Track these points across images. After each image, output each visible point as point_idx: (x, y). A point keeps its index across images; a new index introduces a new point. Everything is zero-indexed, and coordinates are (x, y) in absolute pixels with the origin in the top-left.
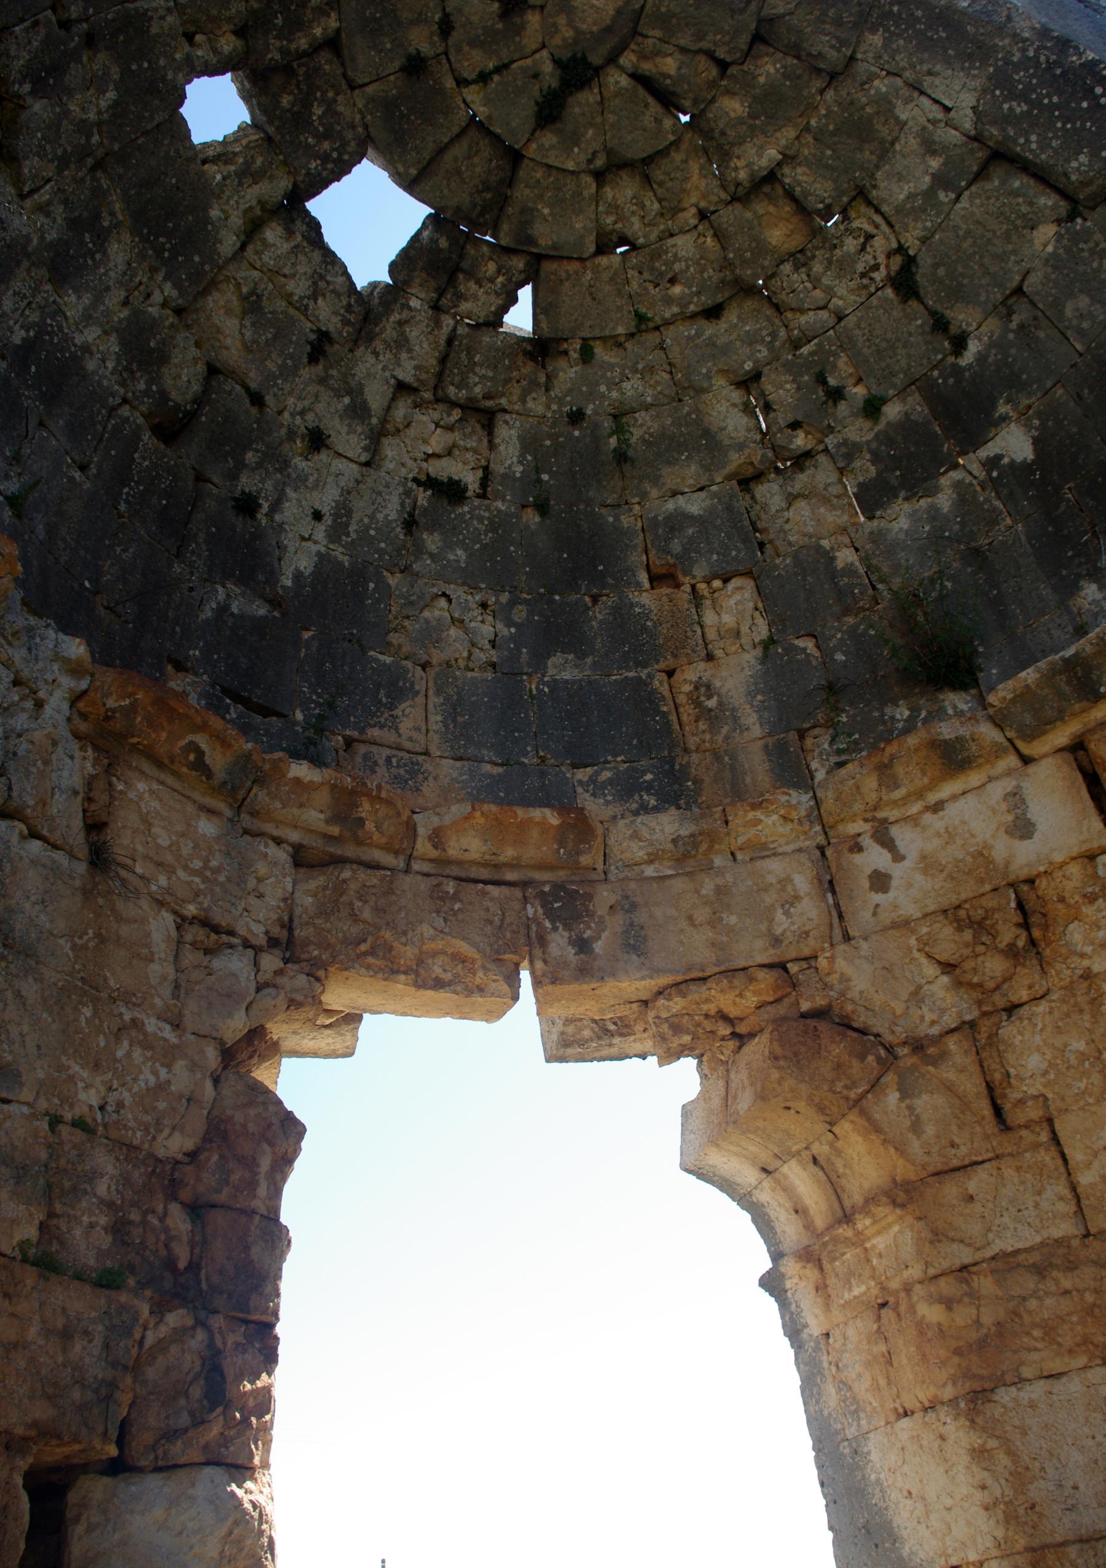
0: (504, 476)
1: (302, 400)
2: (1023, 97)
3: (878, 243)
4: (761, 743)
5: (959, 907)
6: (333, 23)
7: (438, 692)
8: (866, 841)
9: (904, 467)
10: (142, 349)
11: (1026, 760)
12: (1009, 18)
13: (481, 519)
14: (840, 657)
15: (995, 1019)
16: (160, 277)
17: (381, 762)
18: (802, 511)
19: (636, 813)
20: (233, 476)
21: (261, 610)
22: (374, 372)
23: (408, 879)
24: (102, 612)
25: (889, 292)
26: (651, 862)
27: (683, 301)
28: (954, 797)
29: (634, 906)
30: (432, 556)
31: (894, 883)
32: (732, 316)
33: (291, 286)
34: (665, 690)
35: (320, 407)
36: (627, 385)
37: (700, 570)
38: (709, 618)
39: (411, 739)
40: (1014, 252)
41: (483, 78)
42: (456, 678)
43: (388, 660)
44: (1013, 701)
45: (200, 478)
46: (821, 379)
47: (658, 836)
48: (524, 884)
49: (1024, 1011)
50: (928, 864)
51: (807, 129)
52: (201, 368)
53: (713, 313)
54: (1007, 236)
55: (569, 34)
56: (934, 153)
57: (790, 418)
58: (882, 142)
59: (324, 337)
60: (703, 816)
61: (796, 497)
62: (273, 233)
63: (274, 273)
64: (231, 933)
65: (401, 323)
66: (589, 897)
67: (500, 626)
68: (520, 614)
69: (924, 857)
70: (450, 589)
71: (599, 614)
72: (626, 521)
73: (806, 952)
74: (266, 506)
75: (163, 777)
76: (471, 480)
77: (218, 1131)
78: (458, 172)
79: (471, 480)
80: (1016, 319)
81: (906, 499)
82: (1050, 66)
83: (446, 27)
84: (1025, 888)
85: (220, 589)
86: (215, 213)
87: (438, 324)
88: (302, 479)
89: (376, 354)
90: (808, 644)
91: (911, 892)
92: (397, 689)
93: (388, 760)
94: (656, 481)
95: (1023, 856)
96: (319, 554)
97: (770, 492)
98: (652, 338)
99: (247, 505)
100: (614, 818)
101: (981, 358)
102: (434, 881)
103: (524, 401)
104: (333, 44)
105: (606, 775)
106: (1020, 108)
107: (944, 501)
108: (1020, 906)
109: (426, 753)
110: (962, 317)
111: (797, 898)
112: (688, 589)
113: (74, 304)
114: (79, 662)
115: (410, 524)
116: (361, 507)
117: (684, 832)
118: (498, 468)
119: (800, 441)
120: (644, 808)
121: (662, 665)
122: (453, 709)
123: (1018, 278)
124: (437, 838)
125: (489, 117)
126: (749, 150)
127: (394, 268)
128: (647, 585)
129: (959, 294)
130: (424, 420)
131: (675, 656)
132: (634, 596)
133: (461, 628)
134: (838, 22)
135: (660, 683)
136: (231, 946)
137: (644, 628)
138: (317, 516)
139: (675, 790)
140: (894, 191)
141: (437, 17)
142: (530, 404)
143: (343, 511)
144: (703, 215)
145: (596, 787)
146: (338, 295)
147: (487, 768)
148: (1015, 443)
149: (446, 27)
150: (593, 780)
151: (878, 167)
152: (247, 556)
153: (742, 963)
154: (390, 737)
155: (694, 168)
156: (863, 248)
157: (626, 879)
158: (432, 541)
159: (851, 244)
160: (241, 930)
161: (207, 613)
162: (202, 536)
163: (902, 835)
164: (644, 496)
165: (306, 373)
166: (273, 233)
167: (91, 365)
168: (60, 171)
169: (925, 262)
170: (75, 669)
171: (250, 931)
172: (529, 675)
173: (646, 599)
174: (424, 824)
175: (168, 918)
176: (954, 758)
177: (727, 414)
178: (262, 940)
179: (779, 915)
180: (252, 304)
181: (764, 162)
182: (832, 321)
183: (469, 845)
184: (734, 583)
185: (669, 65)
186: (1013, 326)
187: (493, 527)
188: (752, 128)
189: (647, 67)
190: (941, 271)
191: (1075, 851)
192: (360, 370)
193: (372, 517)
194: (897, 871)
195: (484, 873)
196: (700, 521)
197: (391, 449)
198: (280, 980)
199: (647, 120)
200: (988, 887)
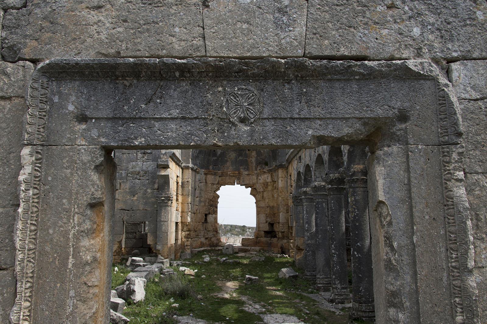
77: (214, 197)
91: (261, 181)
92: (227, 161)
139: (248, 169)
145: (242, 168)
176: (265, 172)
194: (261, 179)
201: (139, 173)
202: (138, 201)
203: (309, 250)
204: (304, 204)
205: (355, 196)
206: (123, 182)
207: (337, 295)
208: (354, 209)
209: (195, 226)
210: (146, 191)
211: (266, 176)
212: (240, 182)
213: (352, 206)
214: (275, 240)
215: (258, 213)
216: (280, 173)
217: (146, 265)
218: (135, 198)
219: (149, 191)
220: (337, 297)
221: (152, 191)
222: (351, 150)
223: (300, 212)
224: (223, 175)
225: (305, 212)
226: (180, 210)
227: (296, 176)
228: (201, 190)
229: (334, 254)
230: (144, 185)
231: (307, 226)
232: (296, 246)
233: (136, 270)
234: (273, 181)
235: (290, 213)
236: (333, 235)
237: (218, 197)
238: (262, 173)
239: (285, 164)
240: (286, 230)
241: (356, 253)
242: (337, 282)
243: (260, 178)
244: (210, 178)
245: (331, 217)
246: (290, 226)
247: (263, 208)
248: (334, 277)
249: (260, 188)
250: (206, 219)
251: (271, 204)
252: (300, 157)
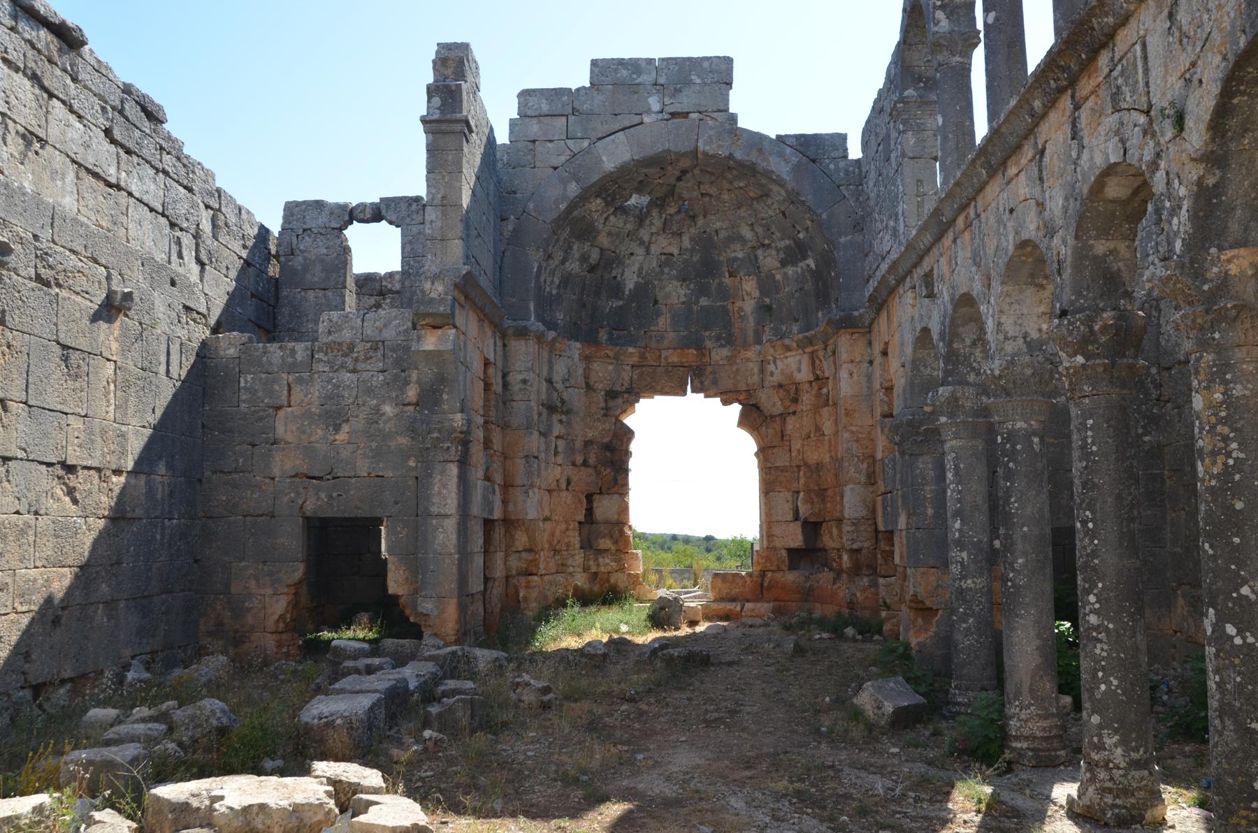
10: (584, 258)
18: (769, 259)
21: (621, 303)
22: (644, 234)
37: (742, 274)
50: (782, 373)
62: (612, 218)
68: (692, 286)
76: (676, 251)
77: (615, 435)
79: (676, 251)
97: (759, 252)
107: (799, 270)
119: (767, 242)
120: (722, 346)
124: (666, 358)
133: (675, 292)
135: (730, 307)
143: (641, 269)
145: (710, 337)
148: (811, 262)
152: (616, 290)
158: (666, 270)
163: (778, 362)
166: (612, 218)
173: (727, 280)
174: (664, 353)
177: (747, 233)
180: (609, 234)
183: (675, 359)
194: (777, 372)
197: (653, 248)
201: (351, 347)
202: (351, 448)
203: (965, 614)
204: (947, 446)
205: (1227, 383)
206: (300, 381)
207: (1110, 791)
208: (1225, 439)
209: (553, 534)
210: (377, 410)
212: (702, 383)
213: (1213, 427)
214: (825, 577)
215: (769, 487)
216: (845, 344)
217: (380, 668)
218: (342, 437)
219: (388, 409)
220: (1109, 799)
221: (396, 411)
222: (1211, 181)
223: (924, 478)
225: (950, 475)
226: (498, 478)
227: (909, 350)
229: (1096, 628)
230: (370, 391)
231: (957, 525)
232: (908, 598)
233: (337, 686)
234: (817, 379)
235: (881, 483)
236: (1094, 554)
237: (628, 434)
239: (861, 316)
240: (866, 545)
241: (1231, 629)
242: (1109, 741)
243: (771, 367)
245: (1084, 485)
246: (881, 527)
247: (783, 469)
248: (1096, 719)
249: (772, 402)
250: (590, 511)
251: (813, 457)
252: (928, 278)
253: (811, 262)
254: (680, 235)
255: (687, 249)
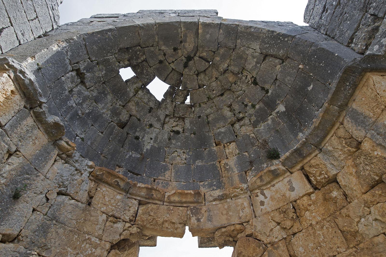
0: (187, 129)
1: (149, 119)
2: (268, 43)
3: (248, 76)
4: (237, 174)
5: (279, 209)
6: (145, 57)
7: (174, 169)
8: (259, 194)
9: (262, 117)
10: (115, 113)
11: (291, 173)
12: (262, 30)
13: (183, 137)
14: (252, 156)
15: (290, 237)
16: (118, 101)
17: (161, 183)
18: (244, 128)
19: (212, 191)
20: (134, 133)
22: (161, 114)
23: (163, 206)
24: (102, 157)
25: (252, 85)
26: (214, 201)
27: (216, 94)
28: (277, 183)
29: (210, 211)
30: (174, 144)
31: (265, 203)
32: (225, 95)
33: (144, 100)
34: (219, 165)
35: (151, 120)
36: (208, 110)
38: (227, 151)
39: (167, 178)
40: (273, 72)
41: (173, 62)
42: (177, 166)
43: (165, 164)
44: (285, 160)
45: (128, 134)
46: (243, 103)
47: (215, 195)
48: (187, 207)
49: (297, 235)
50: (272, 198)
51: (231, 59)
52: (128, 115)
53: (222, 95)
54: (272, 69)
55: (186, 52)
56: (254, 58)
57: (238, 111)
58: (245, 58)
59: (151, 108)
60: (225, 190)
61: (242, 126)
63: (141, 99)
64: (120, 219)
65: (166, 105)
66: (201, 209)
67: (187, 156)
68: (191, 153)
69: (271, 197)
70: (177, 150)
71: (206, 152)
72: (210, 134)
73: (247, 220)
74: (141, 138)
75: (110, 187)
76: (181, 130)
78: (172, 78)
79: (181, 130)
80: (277, 84)
81: (262, 123)
82: (271, 36)
83: (165, 55)
84: (294, 203)
85: (130, 153)
86: (128, 90)
87: (172, 104)
88: (148, 132)
89: (161, 110)
90: (246, 154)
91: (269, 205)
92: (165, 169)
93: (162, 183)
94: (215, 126)
95: (293, 195)
96: (151, 145)
97: (237, 126)
98: (211, 101)
99: (137, 138)
100: (207, 192)
101: (272, 93)
102: (168, 207)
103: (190, 115)
104: (145, 60)
105: (207, 183)
106: (268, 45)
107: (270, 122)
108: (294, 207)
109: (171, 181)
110: (267, 87)
111: (245, 208)
112: (223, 145)
113: (100, 106)
114: (91, 166)
115: (170, 139)
116: (160, 137)
117: (220, 194)
118: (186, 128)
119: (241, 115)
120: (213, 190)
121: (218, 161)
122: (176, 172)
123: (275, 77)
125: (175, 68)
126: (222, 65)
127: (164, 96)
128: (215, 146)
129: (265, 82)
130: (172, 120)
131: (220, 159)
132: (212, 148)
133: (179, 157)
134: (232, 40)
136: (120, 221)
137: (215, 154)
138: (151, 139)
139: (220, 186)
140: (249, 67)
141: (163, 53)
142: (191, 116)
143: (156, 138)
144: (216, 78)
145: (204, 186)
146: (153, 101)
147: (182, 183)
148: (281, 108)
149: (165, 55)
150: (204, 184)
151: (245, 63)
153: (233, 223)
154: (163, 178)
155: (214, 71)
156: (246, 78)
157: (209, 205)
159: (244, 78)
160: (122, 217)
161: (127, 157)
162: (127, 144)
164: (213, 129)
165: (148, 115)
167: (104, 116)
168: (95, 84)
169: (258, 78)
170: (91, 167)
171: (124, 217)
172: (192, 165)
174: (167, 194)
175: (104, 216)
176: (275, 175)
178: (128, 220)
179: (241, 212)
180: (137, 104)
181: (225, 67)
182: (243, 92)
184: (231, 144)
185: (205, 54)
186: (277, 86)
187: (185, 138)
188: (221, 62)
189: (201, 55)
190: (261, 79)
191: (304, 193)
192: (159, 113)
193: (162, 138)
194: (266, 201)
195: (179, 205)
196: (224, 133)
197: (166, 126)
198: (130, 229)
199: (203, 64)
200: (286, 203)
211: (281, 185)
224: (150, 197)
228: (54, 218)
238: (266, 179)
244: (108, 198)
253: (281, 108)
254: (183, 119)
255: (188, 129)
